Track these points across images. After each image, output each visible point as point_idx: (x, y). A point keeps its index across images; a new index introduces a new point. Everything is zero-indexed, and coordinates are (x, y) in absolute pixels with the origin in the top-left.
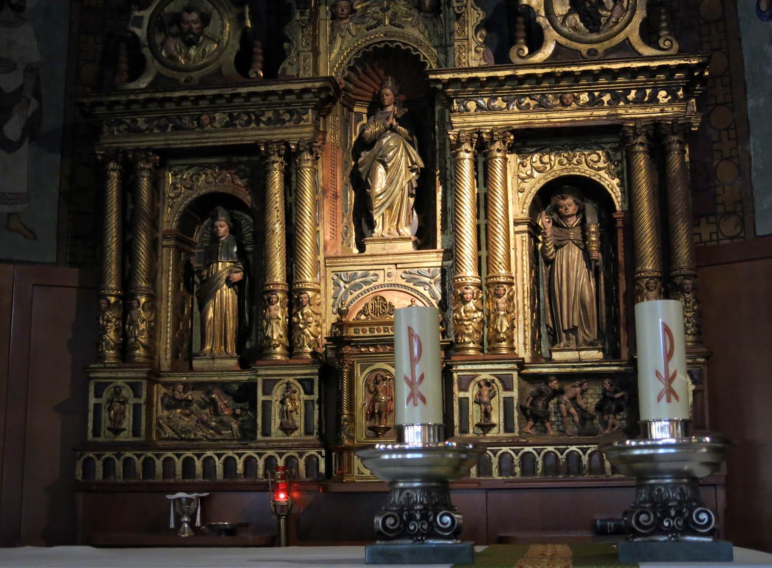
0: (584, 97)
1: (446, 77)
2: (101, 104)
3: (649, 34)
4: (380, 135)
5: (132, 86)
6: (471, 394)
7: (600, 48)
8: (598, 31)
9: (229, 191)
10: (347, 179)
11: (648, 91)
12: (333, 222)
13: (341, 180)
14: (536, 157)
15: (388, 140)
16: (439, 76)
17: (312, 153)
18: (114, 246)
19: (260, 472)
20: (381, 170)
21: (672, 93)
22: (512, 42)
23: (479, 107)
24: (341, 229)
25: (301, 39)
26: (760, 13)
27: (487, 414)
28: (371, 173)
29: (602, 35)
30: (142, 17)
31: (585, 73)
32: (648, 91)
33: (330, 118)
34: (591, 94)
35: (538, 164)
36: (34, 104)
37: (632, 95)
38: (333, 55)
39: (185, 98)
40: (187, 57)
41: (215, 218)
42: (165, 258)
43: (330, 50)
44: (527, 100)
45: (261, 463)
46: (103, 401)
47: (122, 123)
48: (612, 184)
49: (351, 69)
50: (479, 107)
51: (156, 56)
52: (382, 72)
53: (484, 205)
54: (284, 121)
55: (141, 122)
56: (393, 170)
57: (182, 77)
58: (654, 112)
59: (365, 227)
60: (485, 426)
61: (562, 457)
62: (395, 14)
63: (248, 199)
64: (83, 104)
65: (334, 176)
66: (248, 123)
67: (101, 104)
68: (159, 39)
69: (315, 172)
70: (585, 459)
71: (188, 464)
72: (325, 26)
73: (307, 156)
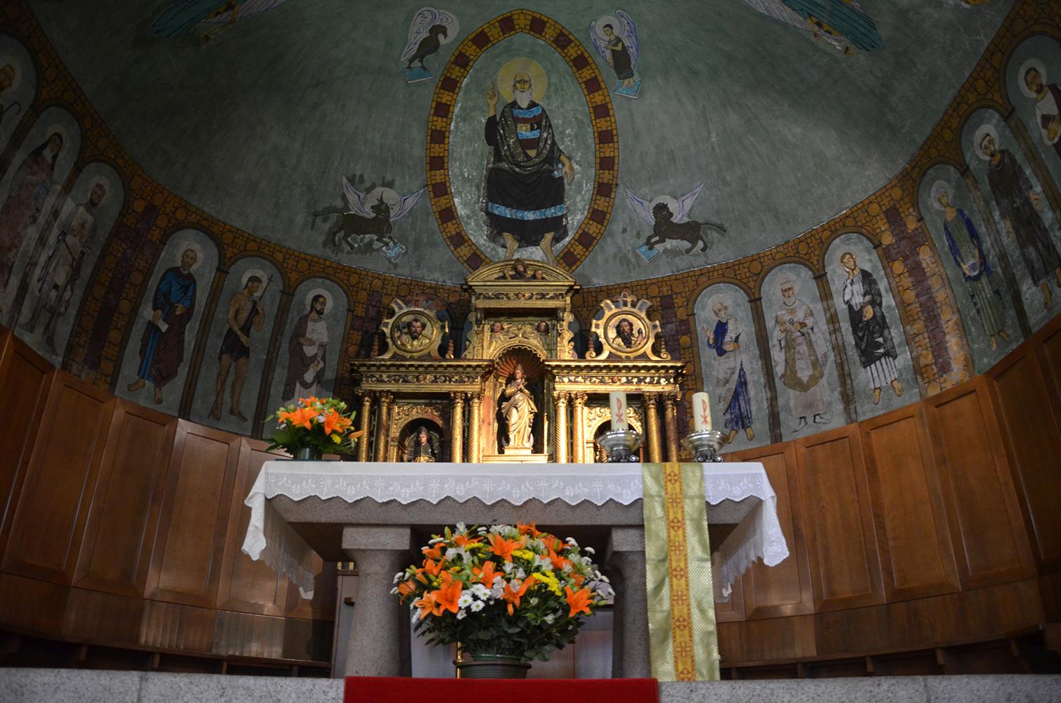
0: (624, 380)
1: (554, 364)
2: (364, 365)
3: (656, 350)
4: (514, 394)
7: (632, 355)
8: (630, 347)
9: (430, 418)
10: (494, 416)
11: (656, 379)
12: (488, 438)
13: (492, 416)
14: (598, 409)
15: (519, 396)
16: (550, 363)
17: (479, 399)
18: (365, 442)
20: (514, 410)
21: (668, 380)
22: (587, 349)
23: (570, 381)
24: (491, 442)
25: (475, 339)
26: (709, 345)
28: (508, 412)
29: (632, 349)
30: (388, 323)
31: (625, 367)
32: (656, 379)
33: (487, 383)
34: (627, 377)
35: (599, 413)
36: (321, 365)
37: (648, 380)
38: (491, 350)
39: (412, 366)
40: (412, 345)
41: (419, 433)
42: (392, 451)
43: (489, 348)
44: (594, 379)
47: (373, 376)
49: (500, 358)
50: (570, 381)
51: (394, 343)
52: (514, 362)
53: (571, 433)
54: (465, 382)
55: (385, 377)
56: (521, 412)
57: (408, 355)
58: (658, 389)
59: (504, 442)
62: (524, 333)
63: (440, 422)
64: (355, 365)
65: (489, 413)
66: (445, 381)
67: (364, 365)
68: (397, 335)
69: (479, 410)
72: (487, 334)
73: (476, 400)
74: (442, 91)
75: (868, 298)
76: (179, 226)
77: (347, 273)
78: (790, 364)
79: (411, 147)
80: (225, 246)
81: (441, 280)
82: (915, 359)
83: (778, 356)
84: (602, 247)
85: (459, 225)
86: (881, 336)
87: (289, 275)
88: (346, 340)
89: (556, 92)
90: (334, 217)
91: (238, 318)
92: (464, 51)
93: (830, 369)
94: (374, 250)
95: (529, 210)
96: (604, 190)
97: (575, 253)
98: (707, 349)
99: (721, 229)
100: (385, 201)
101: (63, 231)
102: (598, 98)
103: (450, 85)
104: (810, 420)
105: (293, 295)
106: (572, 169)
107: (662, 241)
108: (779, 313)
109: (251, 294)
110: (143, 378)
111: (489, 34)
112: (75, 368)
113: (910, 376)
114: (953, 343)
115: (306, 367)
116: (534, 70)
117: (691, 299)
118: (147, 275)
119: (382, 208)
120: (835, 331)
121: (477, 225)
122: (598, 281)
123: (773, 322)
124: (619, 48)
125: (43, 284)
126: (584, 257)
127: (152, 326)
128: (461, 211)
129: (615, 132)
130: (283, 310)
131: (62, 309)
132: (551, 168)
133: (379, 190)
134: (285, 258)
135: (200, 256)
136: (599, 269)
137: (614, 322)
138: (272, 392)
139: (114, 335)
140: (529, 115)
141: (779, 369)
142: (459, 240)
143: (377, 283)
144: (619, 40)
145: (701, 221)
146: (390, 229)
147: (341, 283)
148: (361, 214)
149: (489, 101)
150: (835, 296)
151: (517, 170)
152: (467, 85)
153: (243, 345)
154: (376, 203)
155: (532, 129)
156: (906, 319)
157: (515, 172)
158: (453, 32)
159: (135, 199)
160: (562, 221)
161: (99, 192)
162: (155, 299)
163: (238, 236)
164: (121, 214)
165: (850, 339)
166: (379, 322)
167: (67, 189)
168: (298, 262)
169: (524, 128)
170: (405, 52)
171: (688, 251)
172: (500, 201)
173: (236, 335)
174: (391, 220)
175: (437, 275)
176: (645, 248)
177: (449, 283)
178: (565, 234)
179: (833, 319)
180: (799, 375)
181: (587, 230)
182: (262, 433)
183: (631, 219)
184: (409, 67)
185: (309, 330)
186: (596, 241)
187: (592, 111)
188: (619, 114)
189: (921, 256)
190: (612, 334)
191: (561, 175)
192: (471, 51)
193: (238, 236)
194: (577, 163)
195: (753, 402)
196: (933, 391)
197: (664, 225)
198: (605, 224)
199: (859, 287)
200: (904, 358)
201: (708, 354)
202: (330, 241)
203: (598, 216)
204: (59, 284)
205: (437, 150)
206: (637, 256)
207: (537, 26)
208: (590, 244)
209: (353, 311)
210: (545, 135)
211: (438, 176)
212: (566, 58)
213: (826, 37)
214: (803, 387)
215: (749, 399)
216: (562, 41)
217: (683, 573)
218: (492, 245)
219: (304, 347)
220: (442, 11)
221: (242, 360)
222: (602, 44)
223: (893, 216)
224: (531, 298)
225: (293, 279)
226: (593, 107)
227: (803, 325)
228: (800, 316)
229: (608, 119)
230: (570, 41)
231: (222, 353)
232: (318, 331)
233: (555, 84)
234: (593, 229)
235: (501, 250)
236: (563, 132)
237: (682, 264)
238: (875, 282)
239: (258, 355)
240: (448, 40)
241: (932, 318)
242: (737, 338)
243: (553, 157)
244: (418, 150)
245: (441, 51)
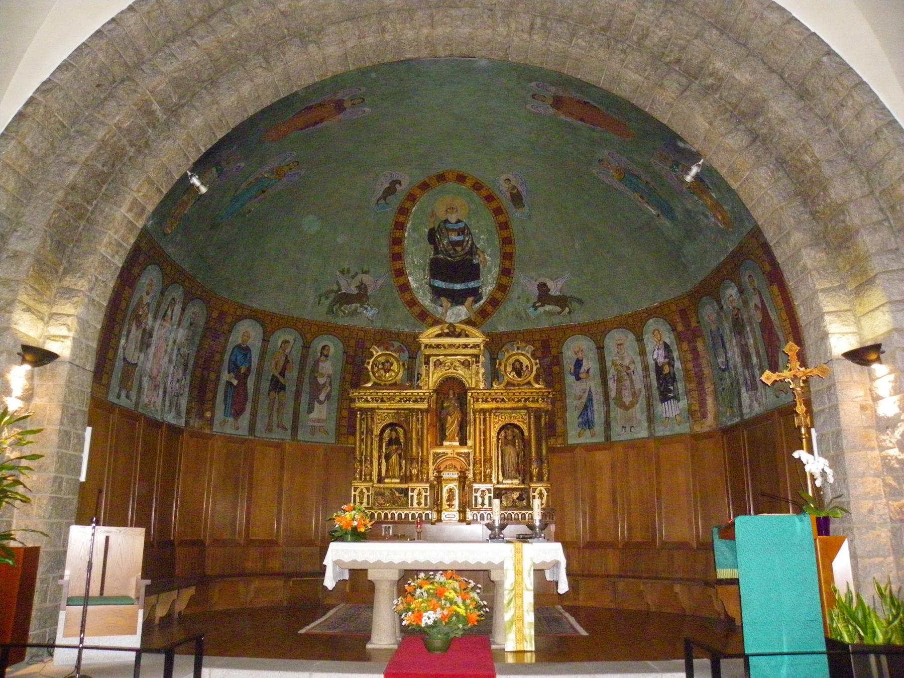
3: (537, 380)
5: (366, 385)
6: (478, 494)
19: (410, 518)
20: (449, 418)
26: (571, 374)
27: (483, 501)
36: (329, 389)
40: (385, 376)
45: (410, 515)
46: (357, 493)
47: (362, 398)
48: (524, 427)
51: (374, 375)
57: (383, 383)
58: (537, 405)
60: (483, 504)
61: (506, 515)
66: (407, 401)
68: (376, 369)
70: (513, 516)
71: (386, 515)
75: (667, 360)
76: (240, 319)
78: (619, 392)
81: (401, 328)
82: (690, 405)
83: (612, 385)
85: (412, 293)
86: (673, 385)
88: (344, 370)
90: (332, 296)
91: (278, 367)
93: (642, 400)
94: (358, 313)
95: (457, 283)
96: (506, 272)
98: (570, 376)
99: (580, 302)
100: (364, 282)
102: (501, 219)
103: (404, 211)
104: (628, 429)
106: (485, 258)
107: (543, 305)
108: (615, 358)
109: (284, 351)
112: (191, 422)
113: (686, 414)
114: (710, 401)
115: (320, 391)
116: (459, 202)
117: (561, 342)
119: (362, 287)
120: (647, 376)
121: (424, 293)
122: (502, 329)
123: (611, 364)
124: (515, 191)
127: (229, 384)
128: (413, 285)
130: (304, 357)
133: (359, 277)
135: (252, 334)
136: (502, 323)
137: (512, 360)
139: (209, 395)
141: (613, 394)
142: (412, 303)
143: (361, 334)
144: (514, 187)
145: (568, 295)
146: (368, 298)
148: (349, 292)
150: (648, 354)
151: (449, 259)
152: (415, 210)
153: (282, 384)
156: (687, 378)
158: (406, 183)
160: (478, 291)
162: (229, 366)
165: (655, 383)
166: (363, 363)
167: (179, 325)
171: (559, 313)
173: (277, 378)
174: (369, 294)
175: (399, 325)
176: (532, 309)
177: (407, 330)
178: (481, 298)
179: (646, 368)
180: (624, 399)
183: (523, 290)
184: (377, 204)
185: (320, 368)
188: (515, 227)
189: (698, 344)
190: (509, 369)
194: (488, 255)
195: (595, 413)
196: (698, 429)
197: (544, 295)
199: (662, 352)
200: (683, 403)
201: (570, 379)
202: (331, 311)
203: (502, 288)
205: (397, 249)
206: (526, 314)
207: (461, 178)
208: (497, 304)
210: (467, 239)
213: (646, 205)
214: (627, 408)
215: (593, 410)
216: (477, 186)
217: (521, 596)
218: (433, 305)
219: (319, 379)
221: (282, 393)
222: (505, 189)
223: (683, 313)
224: (459, 347)
227: (628, 368)
228: (627, 362)
230: (482, 187)
231: (270, 391)
232: (327, 367)
234: (499, 295)
235: (440, 309)
236: (479, 238)
237: (556, 321)
238: (671, 351)
239: (291, 388)
240: (401, 188)
241: (700, 383)
242: (588, 370)
243: (473, 251)
244: (384, 249)
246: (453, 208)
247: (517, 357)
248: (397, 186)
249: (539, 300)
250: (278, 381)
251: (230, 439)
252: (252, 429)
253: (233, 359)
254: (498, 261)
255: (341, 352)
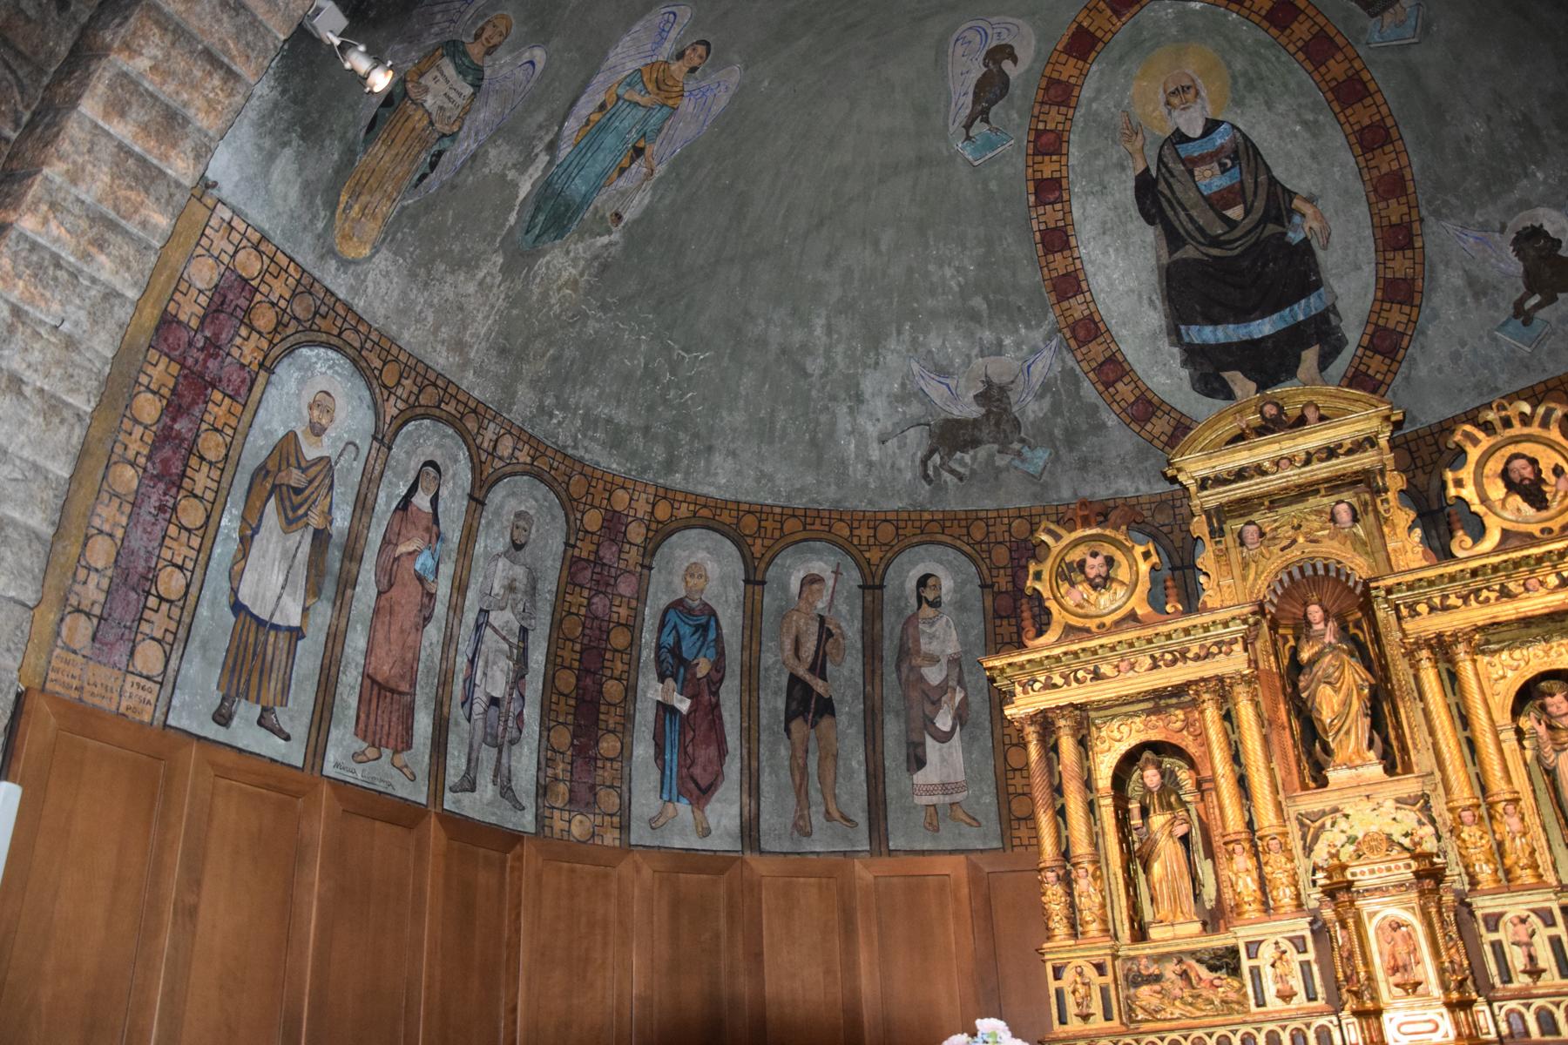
36: (959, 697)
74: (1039, 159)
77: (963, 523)
79: (1014, 275)
80: (750, 541)
84: (1422, 347)
87: (867, 555)
89: (1251, 86)
91: (803, 654)
92: (1055, 75)
97: (1371, 372)
100: (995, 380)
101: (481, 610)
102: (1336, 68)
103: (1048, 144)
105: (881, 587)
110: (670, 801)
111: (1092, 29)
115: (936, 704)
118: (632, 627)
125: (472, 704)
126: (1390, 375)
127: (665, 709)
129: (1389, 122)
130: (872, 616)
131: (515, 733)
132: (1280, 229)
134: (851, 529)
135: (712, 568)
138: (887, 764)
140: (1207, 147)
147: (958, 543)
149: (1128, 146)
151: (1215, 252)
153: (819, 694)
154: (981, 388)
155: (1224, 169)
157: (1215, 257)
158: (1027, 50)
159: (583, 513)
161: (522, 523)
162: (659, 661)
163: (764, 516)
164: (567, 544)
168: (875, 528)
169: (1208, 173)
170: (952, 113)
172: (1199, 319)
181: (1381, 322)
182: (887, 840)
184: (968, 138)
186: (1406, 339)
187: (1330, 95)
188: (1386, 85)
191: (1302, 236)
192: (1068, 70)
193: (764, 516)
198: (1417, 302)
204: (497, 694)
205: (1059, 262)
209: (992, 586)
211: (1078, 308)
212: (1254, 17)
220: (994, 20)
221: (825, 722)
225: (875, 560)
226: (1331, 89)
229: (1368, 101)
231: (788, 720)
233: (1245, 74)
234: (1395, 317)
243: (1279, 204)
245: (1015, 90)
246: (1185, 89)
247: (1512, 449)
248: (1007, 66)
249: (1531, 291)
250: (808, 689)
251: (688, 860)
252: (750, 831)
253: (669, 640)
254: (1361, 211)
255: (974, 587)
